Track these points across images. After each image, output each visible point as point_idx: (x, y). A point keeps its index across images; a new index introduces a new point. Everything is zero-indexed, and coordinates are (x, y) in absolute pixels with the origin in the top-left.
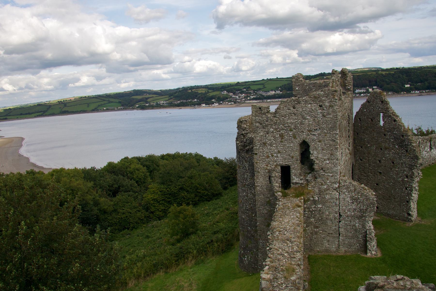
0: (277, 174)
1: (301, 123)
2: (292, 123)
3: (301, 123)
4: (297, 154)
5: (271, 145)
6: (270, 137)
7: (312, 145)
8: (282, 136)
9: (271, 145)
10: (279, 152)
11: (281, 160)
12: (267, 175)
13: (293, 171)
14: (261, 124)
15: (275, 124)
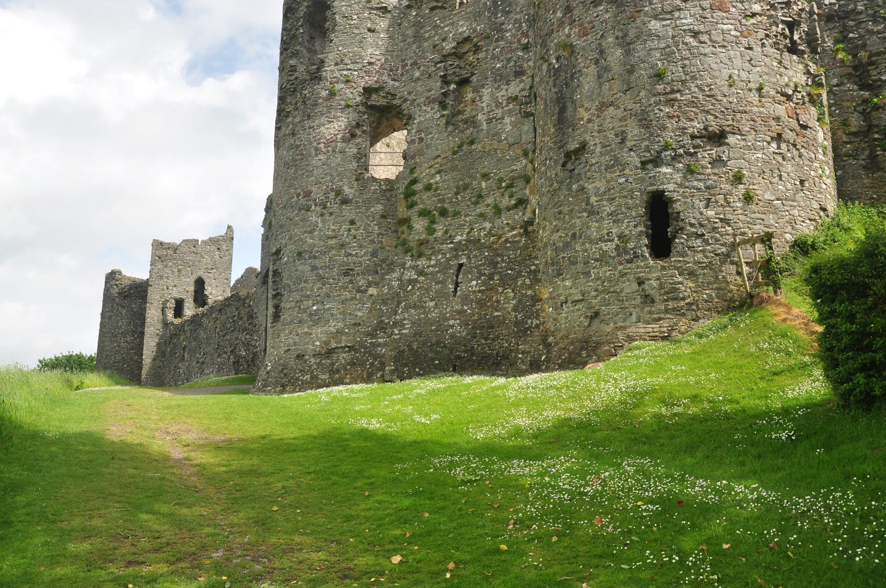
0: (172, 304)
1: (199, 261)
2: (190, 260)
3: (199, 261)
4: (192, 288)
5: (168, 278)
6: (167, 270)
7: (207, 281)
8: (179, 271)
9: (168, 278)
10: (175, 286)
11: (176, 294)
12: (161, 306)
13: (186, 304)
14: (160, 258)
15: (175, 259)
